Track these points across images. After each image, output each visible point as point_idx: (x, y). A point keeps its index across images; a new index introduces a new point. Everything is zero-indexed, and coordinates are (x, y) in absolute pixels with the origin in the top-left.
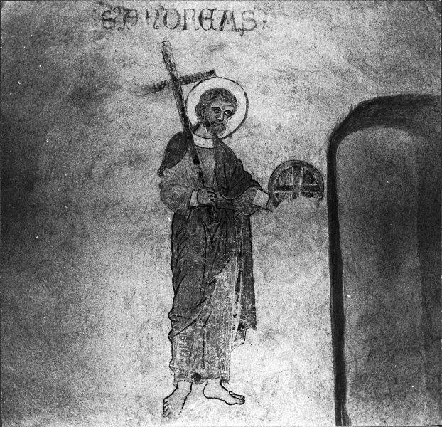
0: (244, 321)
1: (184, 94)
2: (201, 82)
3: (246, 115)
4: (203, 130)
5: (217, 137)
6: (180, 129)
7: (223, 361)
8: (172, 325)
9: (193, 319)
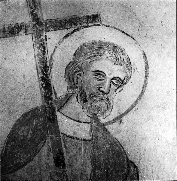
1: (50, 47)
2: (78, 30)
3: (144, 86)
4: (75, 106)
5: (97, 120)
6: (38, 101)
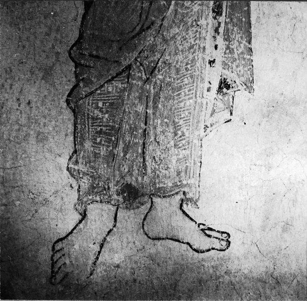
0: (230, 76)
7: (186, 159)
8: (77, 76)
9: (125, 63)
